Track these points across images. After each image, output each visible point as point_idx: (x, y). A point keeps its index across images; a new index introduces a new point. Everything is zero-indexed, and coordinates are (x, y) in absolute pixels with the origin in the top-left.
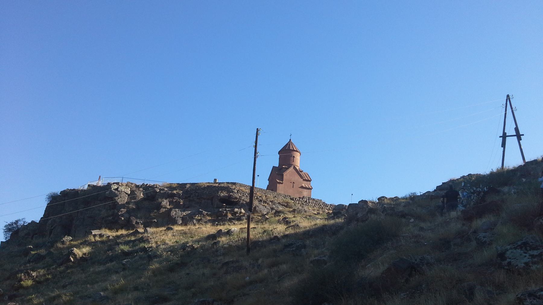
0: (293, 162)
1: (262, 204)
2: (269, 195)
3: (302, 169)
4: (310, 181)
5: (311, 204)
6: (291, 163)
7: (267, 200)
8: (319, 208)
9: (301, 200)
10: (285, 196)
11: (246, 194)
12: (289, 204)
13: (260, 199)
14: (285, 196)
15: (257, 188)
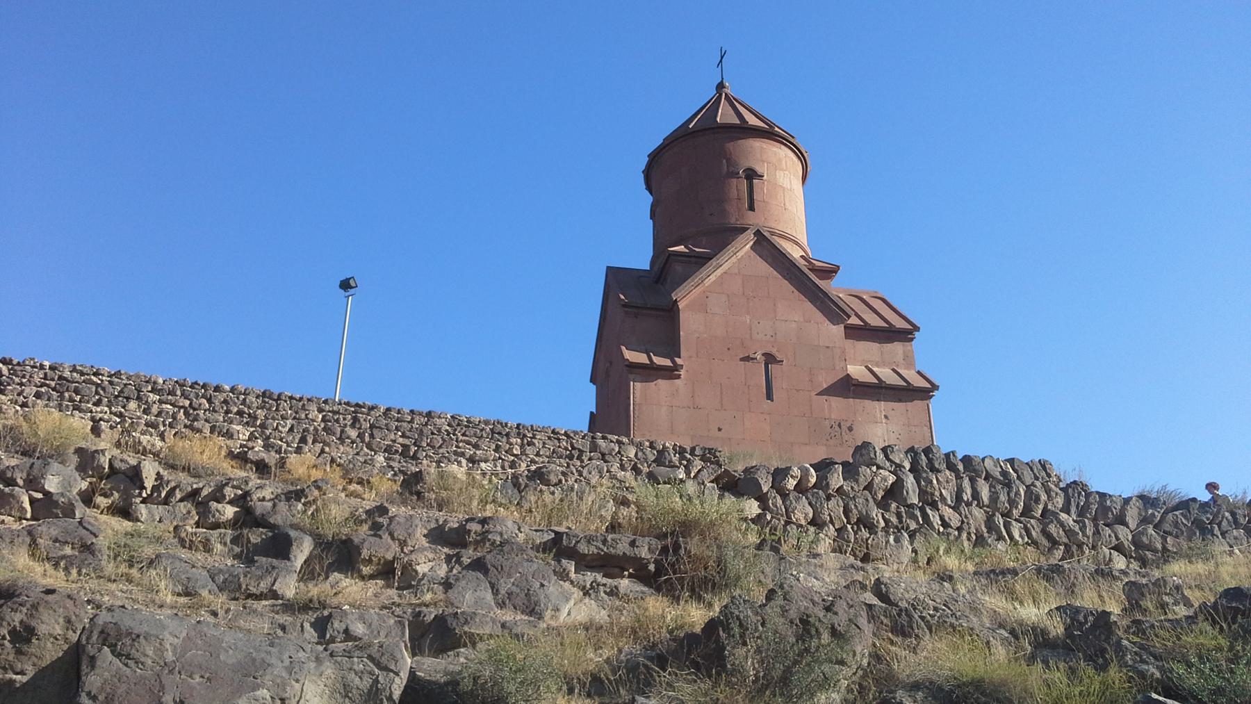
0: (752, 208)
1: (274, 595)
2: (458, 470)
3: (824, 257)
4: (905, 334)
5: (948, 512)
6: (733, 221)
7: (376, 527)
8: (1034, 543)
9: (837, 479)
10: (661, 458)
11: (33, 483)
12: (694, 545)
13: (277, 519)
14: (661, 458)
15: (301, 405)
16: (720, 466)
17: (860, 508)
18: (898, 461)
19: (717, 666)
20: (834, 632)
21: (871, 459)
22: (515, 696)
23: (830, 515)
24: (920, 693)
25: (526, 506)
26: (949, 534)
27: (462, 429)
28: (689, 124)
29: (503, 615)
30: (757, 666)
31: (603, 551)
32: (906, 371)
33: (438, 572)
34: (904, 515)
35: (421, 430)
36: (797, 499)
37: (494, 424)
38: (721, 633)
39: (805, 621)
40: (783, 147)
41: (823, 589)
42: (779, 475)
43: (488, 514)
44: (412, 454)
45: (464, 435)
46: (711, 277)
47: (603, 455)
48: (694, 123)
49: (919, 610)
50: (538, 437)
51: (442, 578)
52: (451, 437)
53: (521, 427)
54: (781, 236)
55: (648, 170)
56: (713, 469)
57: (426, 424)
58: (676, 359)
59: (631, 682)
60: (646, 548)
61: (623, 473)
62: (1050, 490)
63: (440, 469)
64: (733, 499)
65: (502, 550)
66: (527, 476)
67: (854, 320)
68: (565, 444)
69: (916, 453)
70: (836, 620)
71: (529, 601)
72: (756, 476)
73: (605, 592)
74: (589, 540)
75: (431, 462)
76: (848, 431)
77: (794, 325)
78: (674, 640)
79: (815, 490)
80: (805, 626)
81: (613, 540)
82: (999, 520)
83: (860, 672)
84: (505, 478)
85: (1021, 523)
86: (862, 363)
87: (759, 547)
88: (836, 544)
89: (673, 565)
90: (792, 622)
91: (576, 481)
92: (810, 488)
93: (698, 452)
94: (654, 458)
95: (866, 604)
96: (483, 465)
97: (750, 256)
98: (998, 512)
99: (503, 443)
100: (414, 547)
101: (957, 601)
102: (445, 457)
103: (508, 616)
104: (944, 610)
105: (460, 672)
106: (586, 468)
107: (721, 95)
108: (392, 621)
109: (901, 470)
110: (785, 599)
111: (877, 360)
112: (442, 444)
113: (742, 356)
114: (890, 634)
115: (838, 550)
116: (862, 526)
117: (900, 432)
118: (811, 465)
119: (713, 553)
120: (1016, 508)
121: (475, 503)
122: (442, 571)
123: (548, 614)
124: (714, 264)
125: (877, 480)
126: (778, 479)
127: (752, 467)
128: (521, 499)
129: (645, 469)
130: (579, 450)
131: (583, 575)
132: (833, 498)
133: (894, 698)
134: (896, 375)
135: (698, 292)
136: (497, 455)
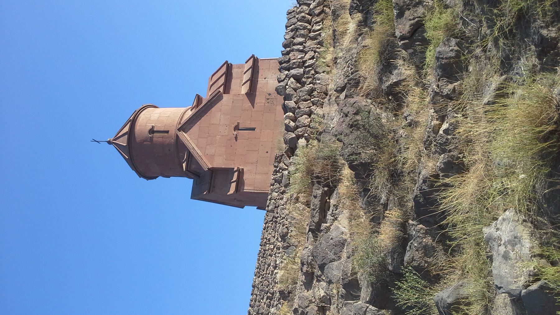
2: (280, 274)
3: (192, 101)
4: (229, 67)
5: (308, 56)
6: (173, 140)
8: (322, 20)
9: (291, 104)
12: (317, 170)
14: (280, 182)
16: (283, 155)
17: (304, 95)
18: (284, 76)
19: (369, 167)
20: (356, 114)
21: (283, 87)
22: (378, 257)
23: (306, 108)
24: (383, 78)
25: (296, 243)
26: (317, 56)
27: (261, 271)
28: (126, 158)
29: (344, 257)
30: (369, 149)
31: (318, 211)
32: (245, 68)
33: (324, 286)
34: (308, 75)
35: (260, 290)
36: (299, 122)
37: (259, 257)
38: (355, 163)
39: (351, 126)
40: (140, 116)
41: (338, 116)
42: (288, 129)
43: (299, 261)
44: (271, 295)
45: (264, 271)
46: (198, 152)
47: (276, 207)
48: (126, 156)
49: (348, 74)
50: (266, 236)
51: (327, 284)
52: (265, 277)
53: (261, 244)
54: (181, 120)
55: (148, 178)
56: (284, 158)
57: (258, 288)
58: (235, 170)
59: (374, 205)
60: (317, 191)
61: (284, 199)
62: (300, 11)
63: (279, 282)
64: (297, 150)
65: (316, 256)
66: (284, 242)
67: (221, 90)
68: (270, 224)
69: (281, 68)
70: (351, 113)
71: (338, 245)
72: (288, 139)
73: (336, 210)
74: (313, 216)
75: (275, 286)
76: (271, 96)
77: (222, 116)
78: (357, 183)
79: (296, 113)
80: (353, 126)
81: (313, 206)
82: (312, 34)
83: (374, 103)
84: (284, 253)
85: (313, 25)
86: (240, 87)
87: (319, 141)
88: (319, 106)
89: (325, 180)
90: (351, 132)
91: (287, 220)
92: (295, 115)
93: (277, 165)
94: (278, 184)
95: (345, 98)
96: (278, 262)
97: (190, 134)
98: (308, 34)
99: (268, 253)
100: (313, 297)
101: (346, 57)
102: (273, 280)
103: (344, 255)
104: (349, 64)
105: (368, 282)
106: (281, 215)
107: (113, 143)
108: (345, 308)
109: (289, 75)
110: (341, 134)
111: (240, 80)
112: (267, 281)
113: (235, 140)
114: (358, 88)
115: (322, 105)
116: (312, 94)
117: (272, 73)
118: (285, 114)
119: (321, 161)
120: (307, 26)
121: (294, 267)
122: (324, 284)
123: (344, 237)
124: (192, 150)
125: (292, 86)
126: (290, 129)
127: (284, 140)
128: (294, 246)
129: (283, 188)
130: (273, 218)
131: (328, 220)
132: (299, 106)
133: (385, 90)
134: (247, 73)
135: (205, 158)
136: (274, 256)
